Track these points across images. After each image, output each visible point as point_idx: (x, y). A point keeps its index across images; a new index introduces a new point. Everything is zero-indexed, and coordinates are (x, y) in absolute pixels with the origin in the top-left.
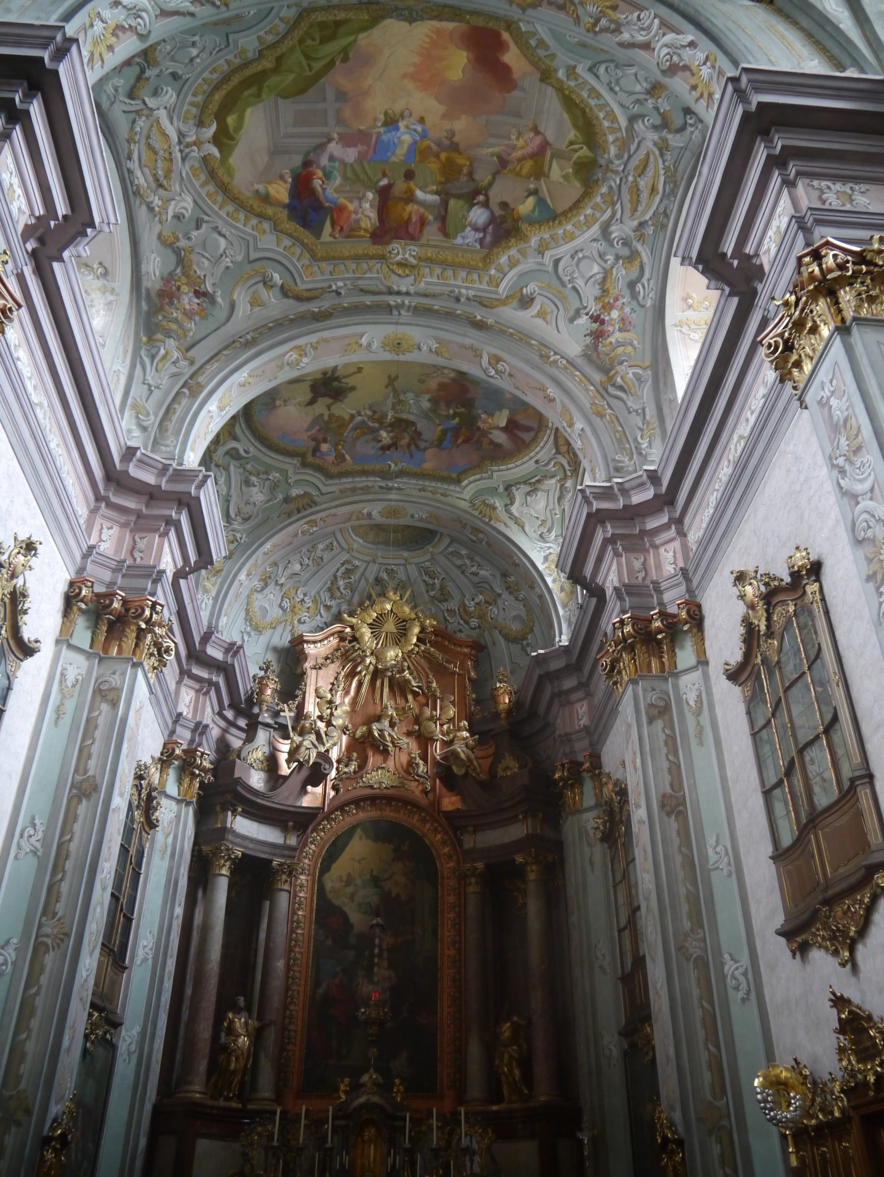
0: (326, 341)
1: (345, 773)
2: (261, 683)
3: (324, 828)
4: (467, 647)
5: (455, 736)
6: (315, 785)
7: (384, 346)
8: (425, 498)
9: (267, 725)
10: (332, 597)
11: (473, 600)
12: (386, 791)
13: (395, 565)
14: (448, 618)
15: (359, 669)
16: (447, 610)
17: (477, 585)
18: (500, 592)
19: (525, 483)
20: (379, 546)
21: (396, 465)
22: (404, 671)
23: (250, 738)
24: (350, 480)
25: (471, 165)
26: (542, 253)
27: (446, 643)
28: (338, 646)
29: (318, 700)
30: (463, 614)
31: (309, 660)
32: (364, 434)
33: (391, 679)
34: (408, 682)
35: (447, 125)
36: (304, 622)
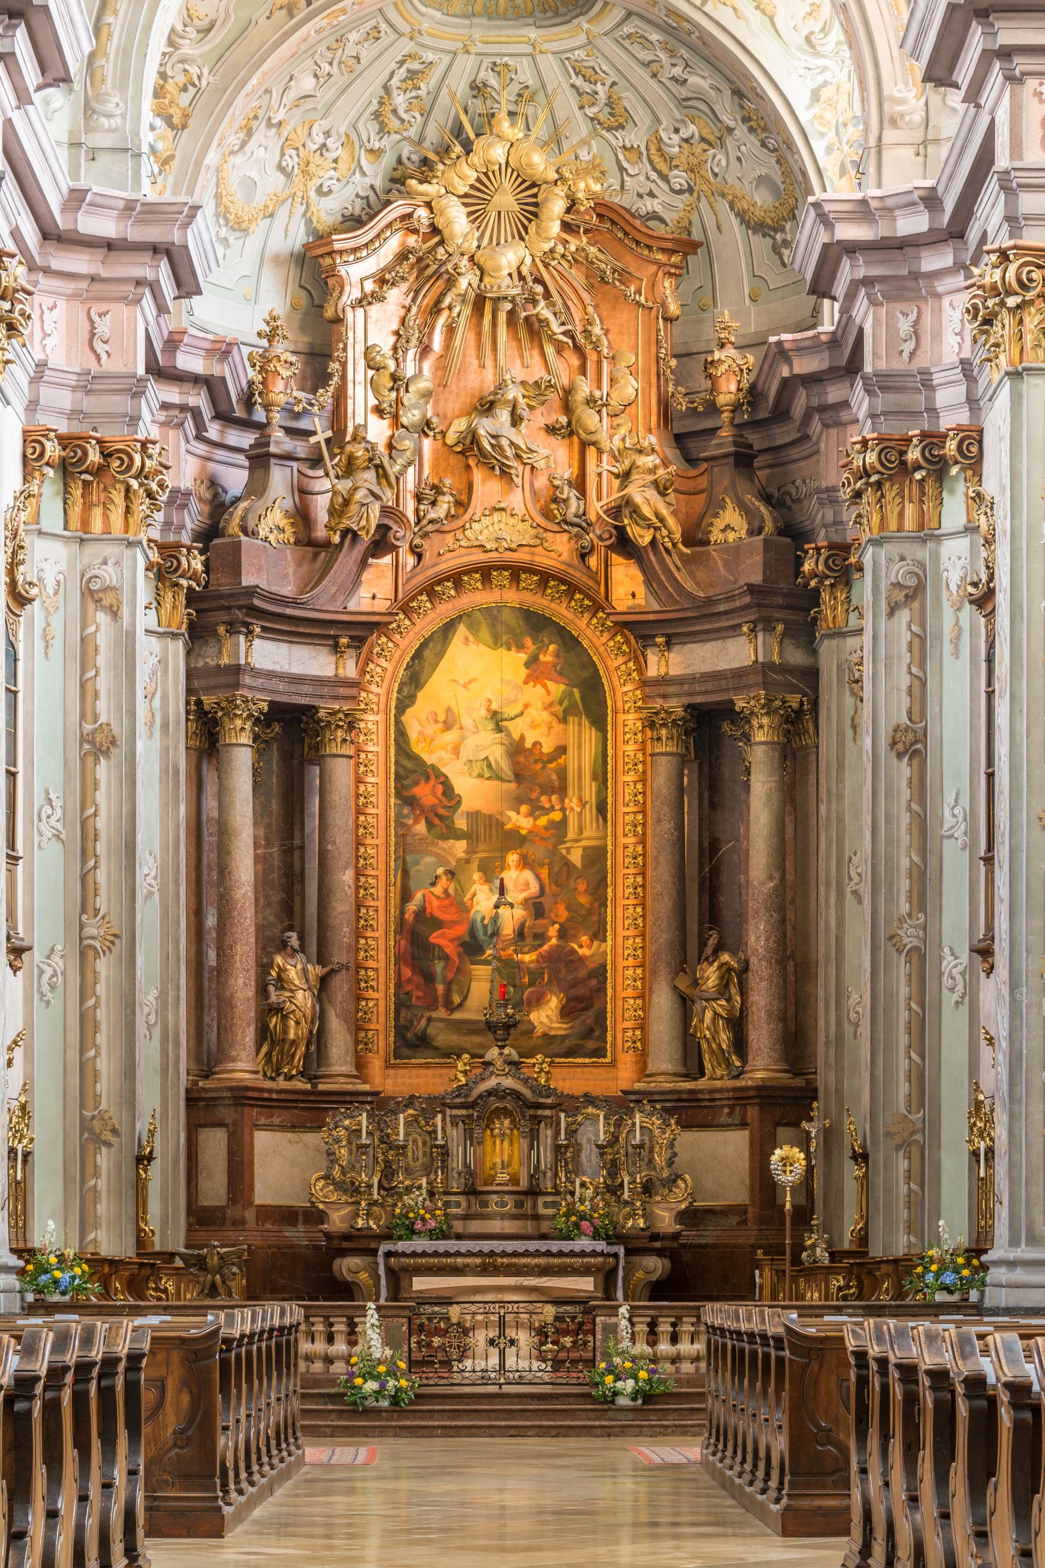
1: (431, 522)
2: (264, 363)
3: (399, 626)
4: (663, 250)
5: (633, 466)
9: (289, 457)
10: (383, 130)
11: (677, 131)
12: (508, 556)
13: (511, 55)
14: (625, 165)
15: (447, 301)
16: (624, 147)
18: (732, 124)
20: (475, 20)
22: (534, 302)
23: (257, 487)
27: (620, 235)
28: (403, 244)
29: (371, 373)
30: (656, 159)
31: (347, 288)
33: (511, 314)
34: (546, 321)
36: (330, 191)
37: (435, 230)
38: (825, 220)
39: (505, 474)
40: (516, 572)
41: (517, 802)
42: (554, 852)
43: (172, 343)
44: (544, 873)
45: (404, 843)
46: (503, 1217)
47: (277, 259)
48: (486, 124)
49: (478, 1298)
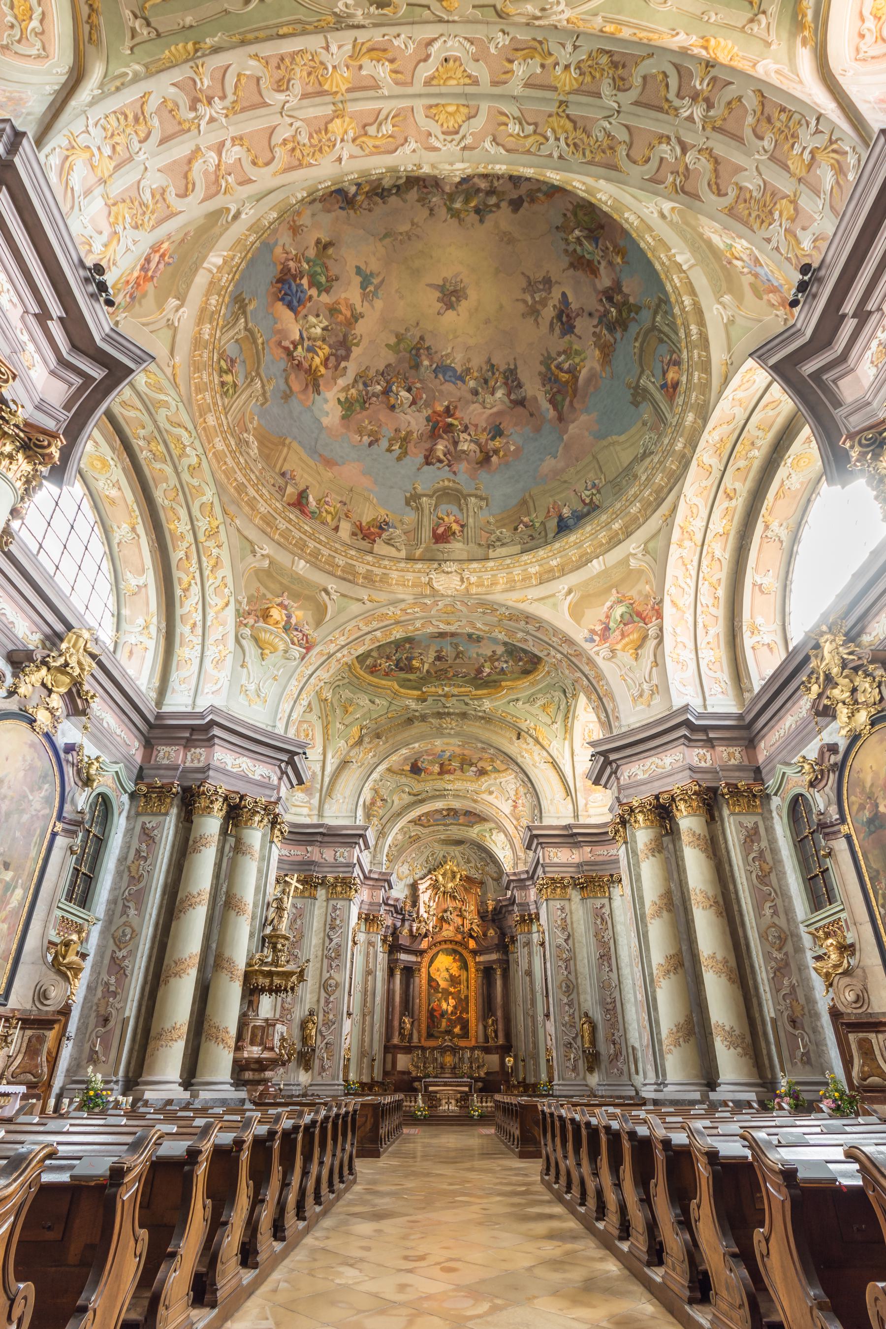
23: (403, 925)
38: (508, 876)
40: (451, 941)
43: (388, 899)
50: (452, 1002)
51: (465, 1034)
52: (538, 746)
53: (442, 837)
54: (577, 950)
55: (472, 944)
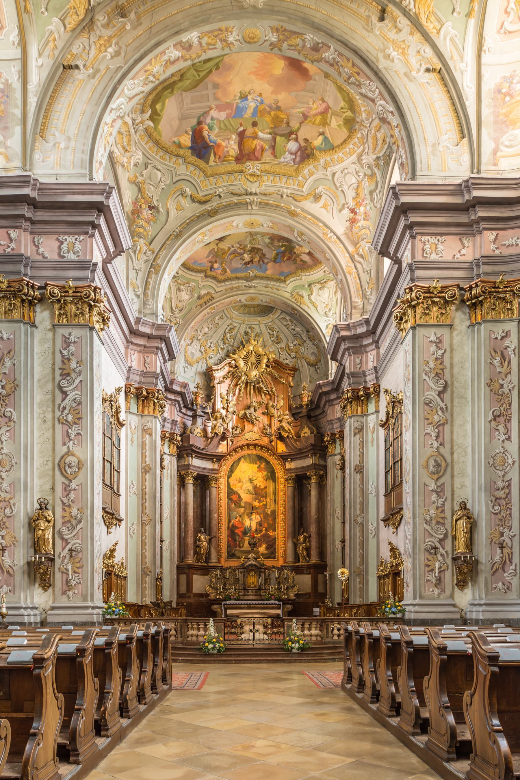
0: (216, 227)
6: (223, 441)
7: (244, 225)
8: (268, 292)
17: (294, 335)
19: (318, 283)
21: (253, 272)
24: (230, 283)
25: (288, 118)
26: (326, 169)
32: (236, 256)
35: (274, 97)
37: (236, 366)
39: (253, 423)
41: (255, 499)
42: (264, 511)
44: (262, 516)
45: (229, 509)
46: (252, 595)
47: (199, 373)
48: (248, 341)
49: (246, 616)
50: (256, 518)
51: (272, 553)
52: (418, 36)
53: (244, 299)
54: (456, 410)
55: (281, 448)
